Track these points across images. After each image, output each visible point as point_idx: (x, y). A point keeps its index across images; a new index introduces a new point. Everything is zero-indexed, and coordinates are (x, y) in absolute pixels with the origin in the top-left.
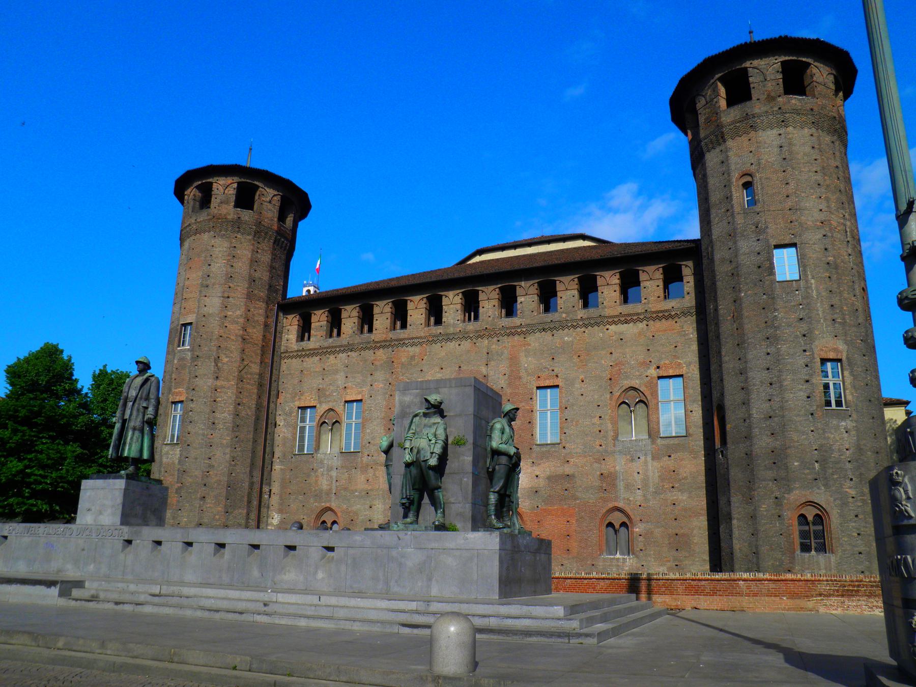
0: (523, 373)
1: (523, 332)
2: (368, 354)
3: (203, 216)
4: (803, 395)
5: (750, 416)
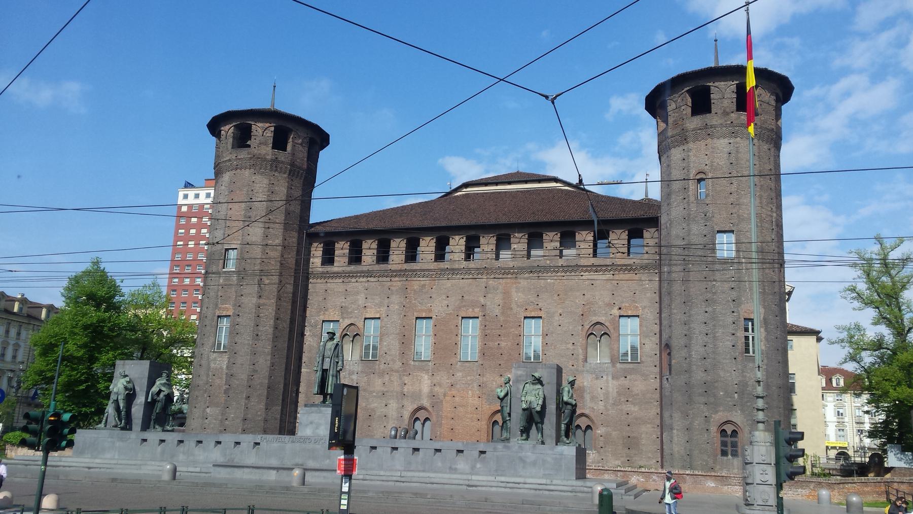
0: (514, 306)
3: (243, 154)
4: (729, 344)
5: (690, 356)
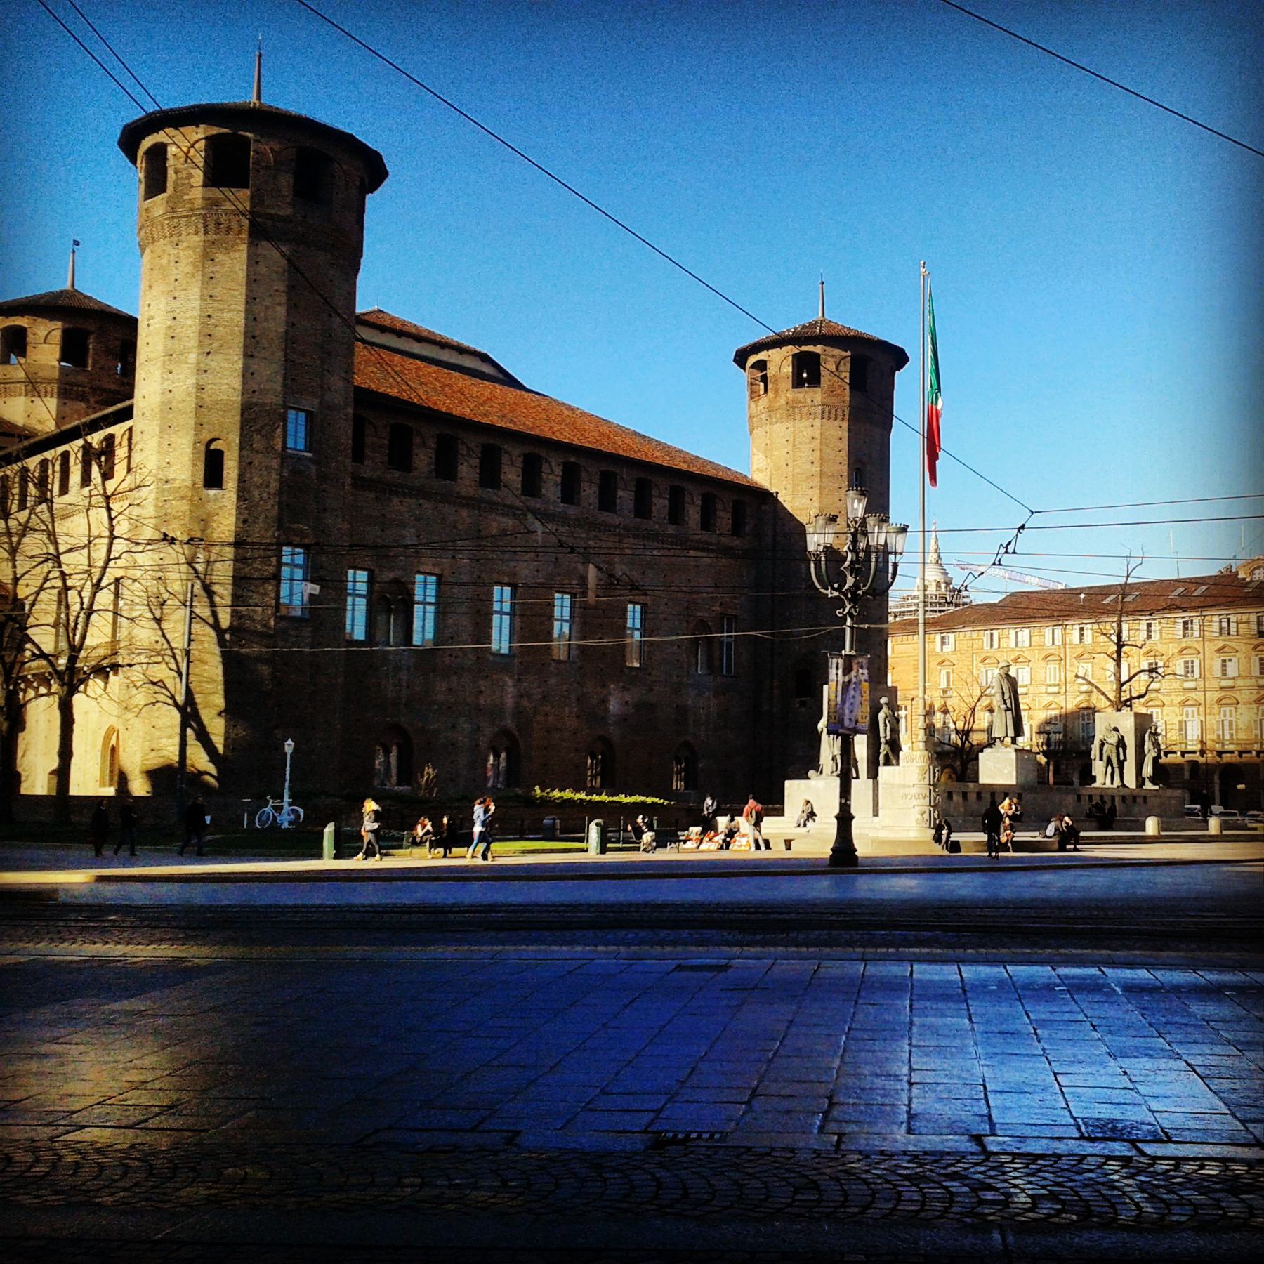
1: (619, 534)
2: (448, 509)
